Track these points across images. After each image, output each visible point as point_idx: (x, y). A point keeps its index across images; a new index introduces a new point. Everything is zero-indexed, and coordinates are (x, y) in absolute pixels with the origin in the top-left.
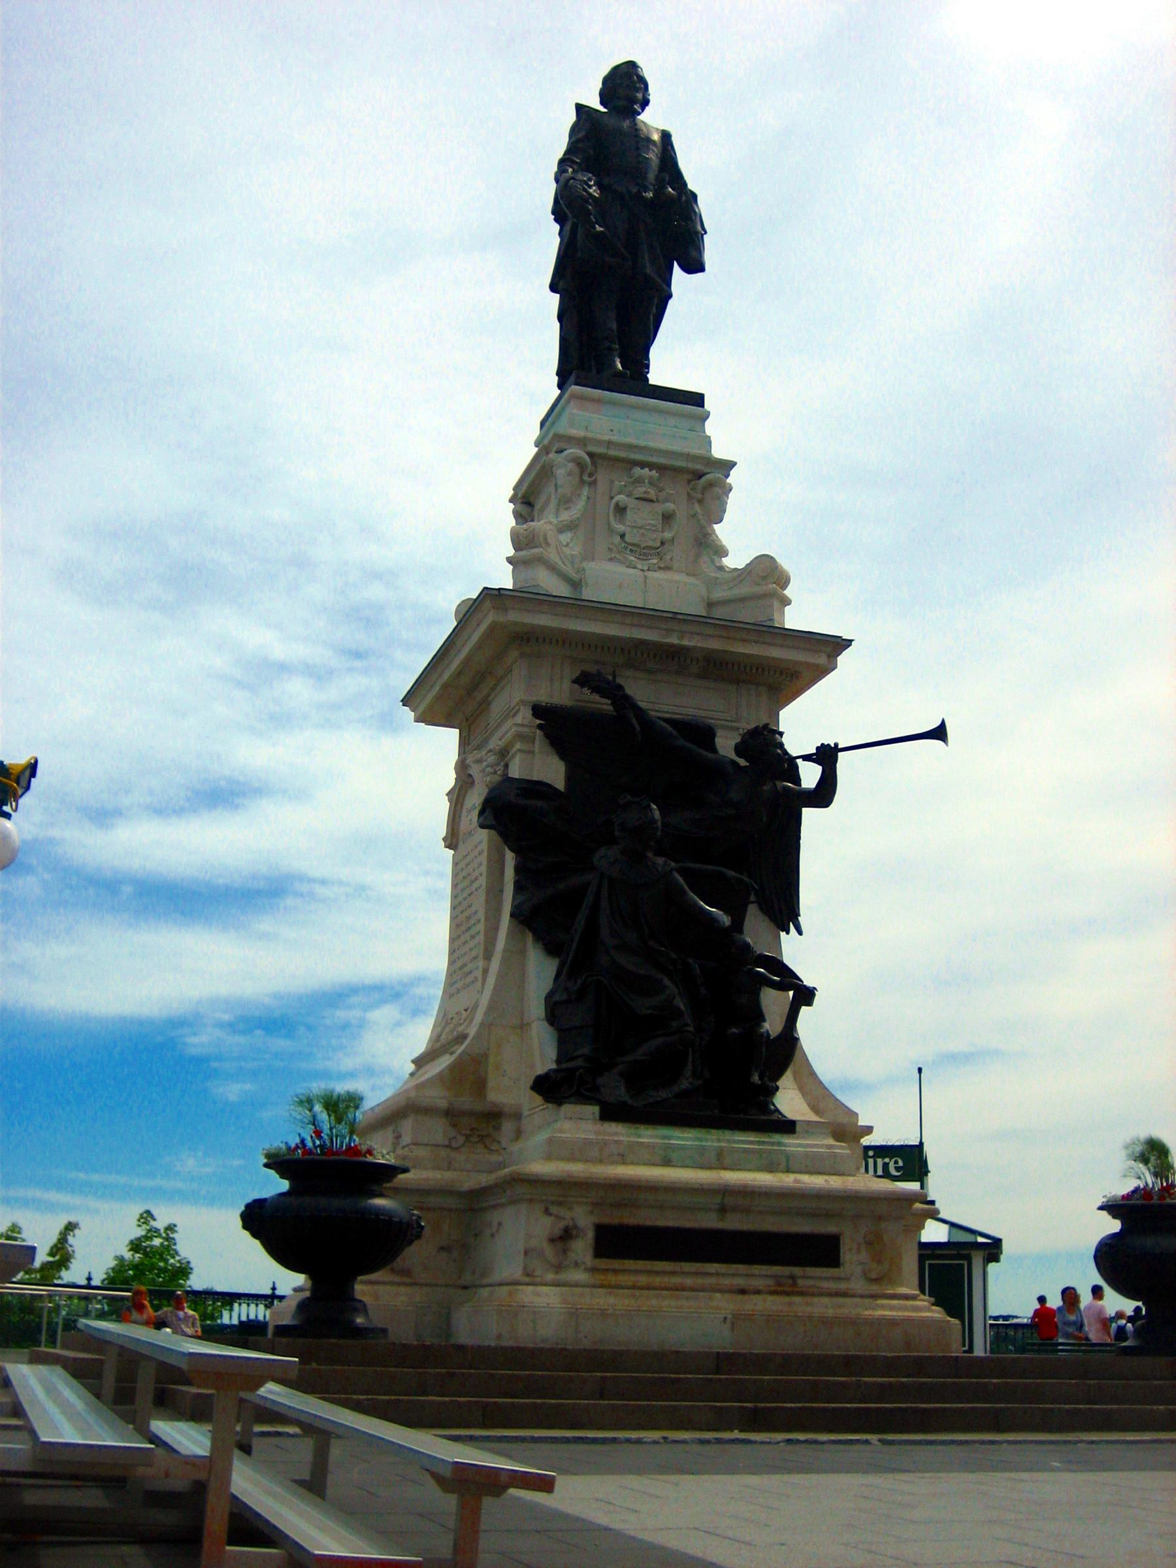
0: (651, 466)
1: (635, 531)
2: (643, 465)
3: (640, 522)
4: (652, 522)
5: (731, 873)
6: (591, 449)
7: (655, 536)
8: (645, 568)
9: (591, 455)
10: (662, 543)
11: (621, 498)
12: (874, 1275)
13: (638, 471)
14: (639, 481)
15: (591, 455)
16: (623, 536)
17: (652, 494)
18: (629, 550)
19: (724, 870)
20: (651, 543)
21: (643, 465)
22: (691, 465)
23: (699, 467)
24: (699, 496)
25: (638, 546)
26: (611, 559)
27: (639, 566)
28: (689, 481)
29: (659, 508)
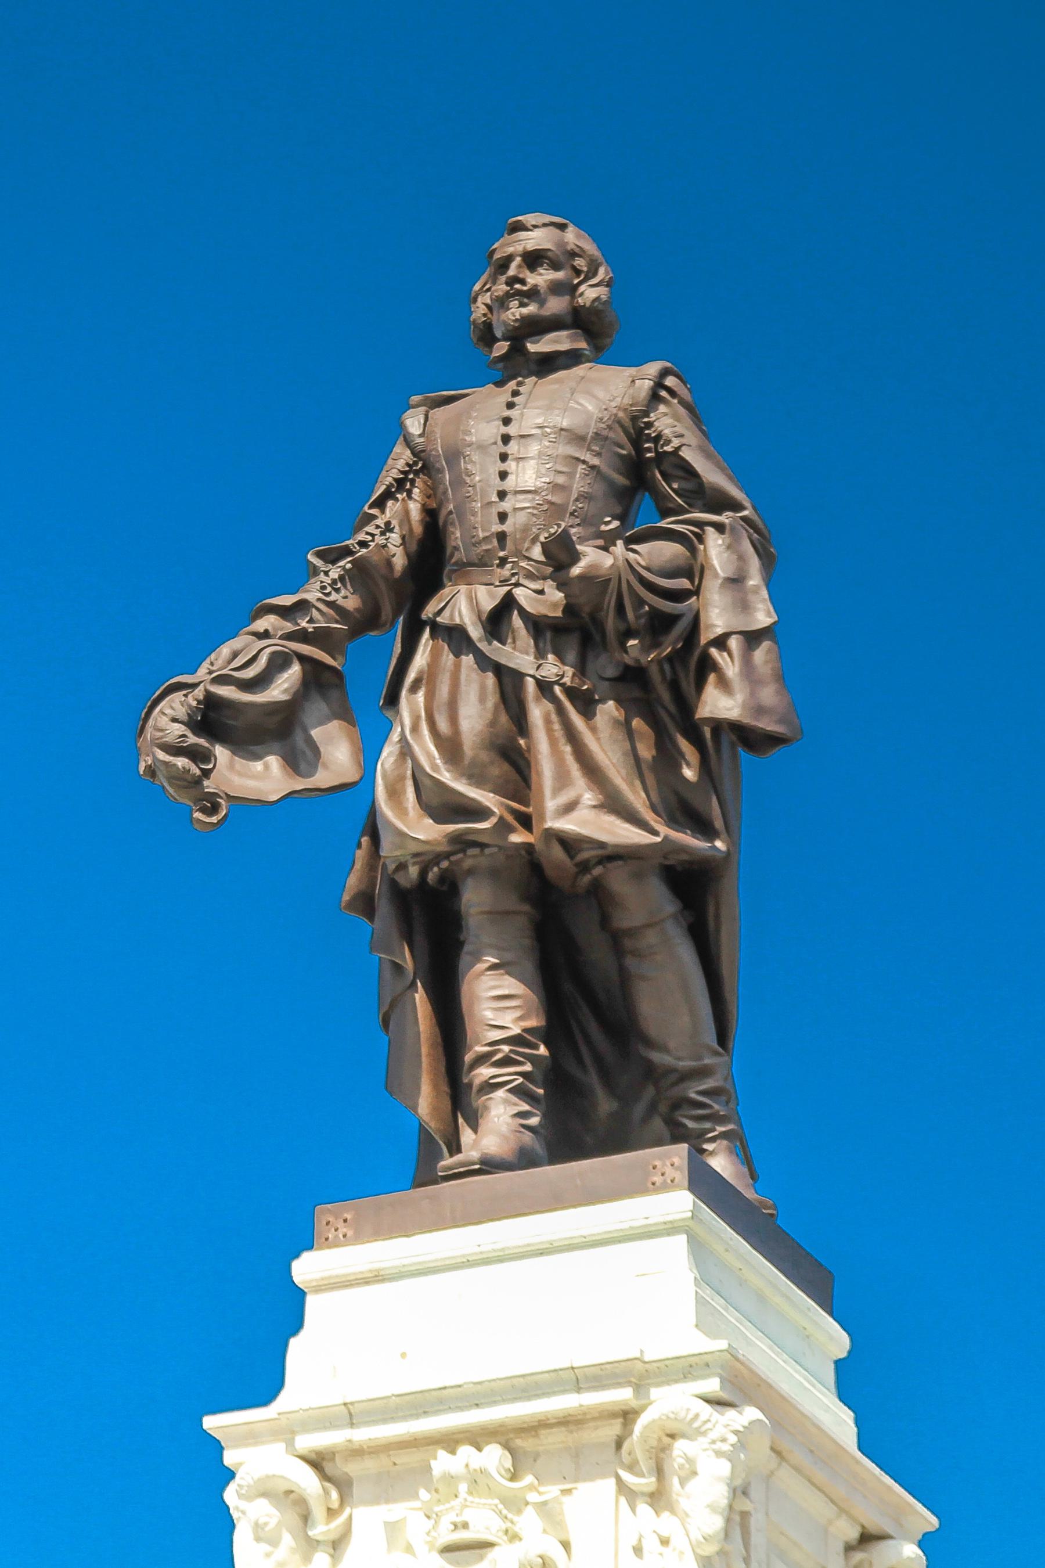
0: (477, 1437)
9: (317, 1462)
13: (442, 1462)
21: (450, 1441)
23: (623, 1395)
24: (645, 1482)
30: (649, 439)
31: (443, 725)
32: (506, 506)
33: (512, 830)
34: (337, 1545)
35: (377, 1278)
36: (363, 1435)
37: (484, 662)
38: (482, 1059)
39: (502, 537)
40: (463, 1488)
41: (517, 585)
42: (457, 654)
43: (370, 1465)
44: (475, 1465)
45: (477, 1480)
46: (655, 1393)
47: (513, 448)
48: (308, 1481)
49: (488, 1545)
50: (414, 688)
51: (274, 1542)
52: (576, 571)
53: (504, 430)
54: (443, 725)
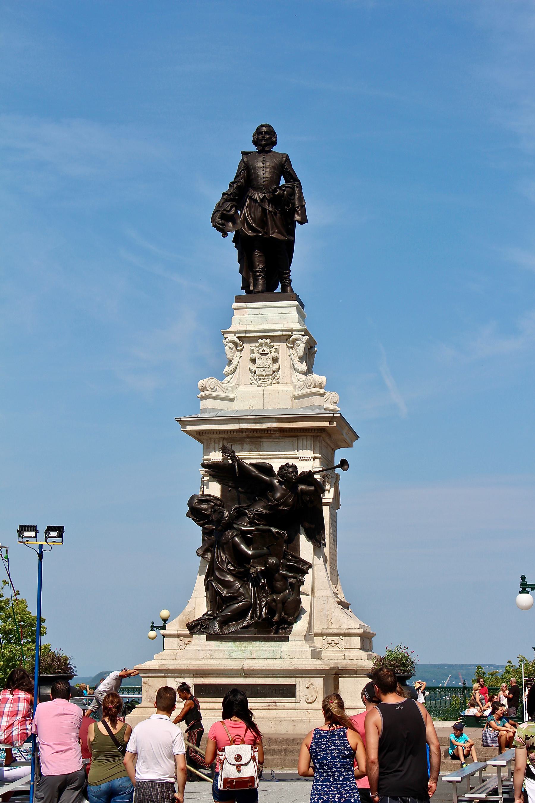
0: (266, 337)
1: (260, 369)
2: (262, 337)
3: (262, 365)
4: (267, 364)
5: (274, 530)
6: (238, 335)
7: (270, 370)
8: (266, 385)
9: (238, 338)
10: (274, 372)
11: (253, 356)
12: (309, 701)
13: (260, 341)
14: (261, 345)
15: (238, 338)
16: (255, 373)
17: (267, 350)
18: (258, 378)
19: (272, 529)
20: (268, 373)
21: (262, 337)
22: (284, 333)
23: (289, 333)
25: (262, 375)
26: (251, 384)
27: (263, 385)
28: (287, 340)
29: (271, 356)
30: (285, 168)
31: (253, 216)
32: (264, 180)
33: (264, 235)
34: (241, 351)
35: (247, 308)
36: (247, 335)
37: (260, 205)
38: (257, 271)
39: (264, 185)
40: (264, 345)
41: (266, 194)
42: (255, 203)
43: (247, 339)
44: (266, 341)
45: (266, 344)
46: (294, 333)
47: (265, 169)
48: (237, 340)
49: (268, 354)
50: (247, 208)
51: (232, 349)
52: (276, 194)
53: (263, 165)
54: (253, 216)
